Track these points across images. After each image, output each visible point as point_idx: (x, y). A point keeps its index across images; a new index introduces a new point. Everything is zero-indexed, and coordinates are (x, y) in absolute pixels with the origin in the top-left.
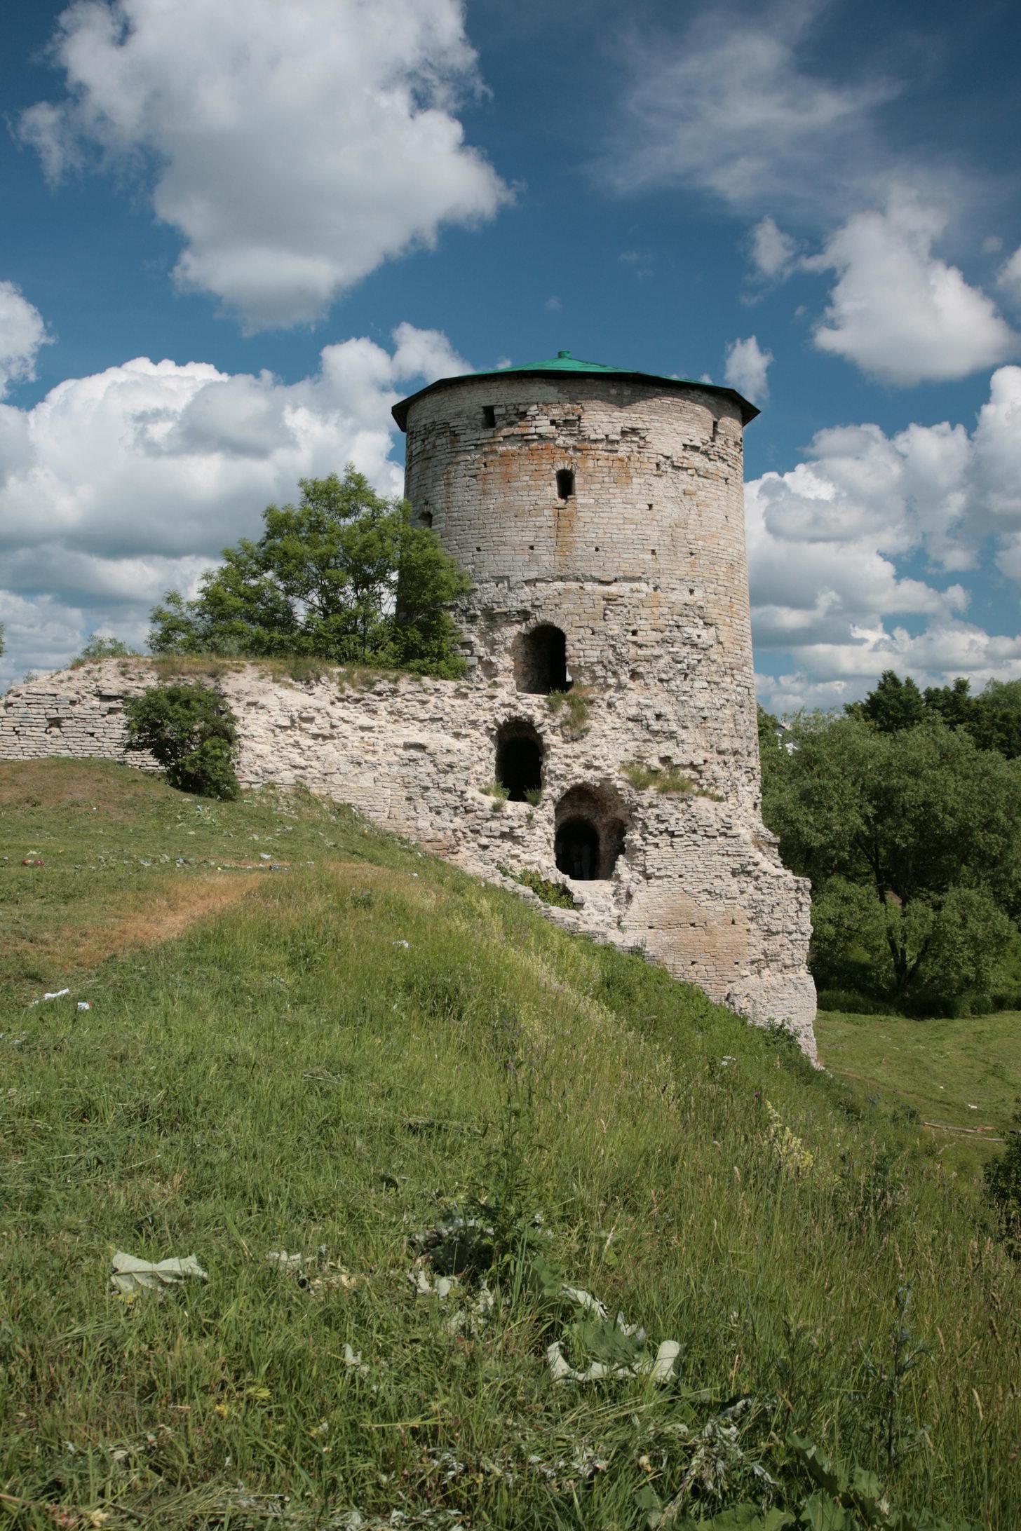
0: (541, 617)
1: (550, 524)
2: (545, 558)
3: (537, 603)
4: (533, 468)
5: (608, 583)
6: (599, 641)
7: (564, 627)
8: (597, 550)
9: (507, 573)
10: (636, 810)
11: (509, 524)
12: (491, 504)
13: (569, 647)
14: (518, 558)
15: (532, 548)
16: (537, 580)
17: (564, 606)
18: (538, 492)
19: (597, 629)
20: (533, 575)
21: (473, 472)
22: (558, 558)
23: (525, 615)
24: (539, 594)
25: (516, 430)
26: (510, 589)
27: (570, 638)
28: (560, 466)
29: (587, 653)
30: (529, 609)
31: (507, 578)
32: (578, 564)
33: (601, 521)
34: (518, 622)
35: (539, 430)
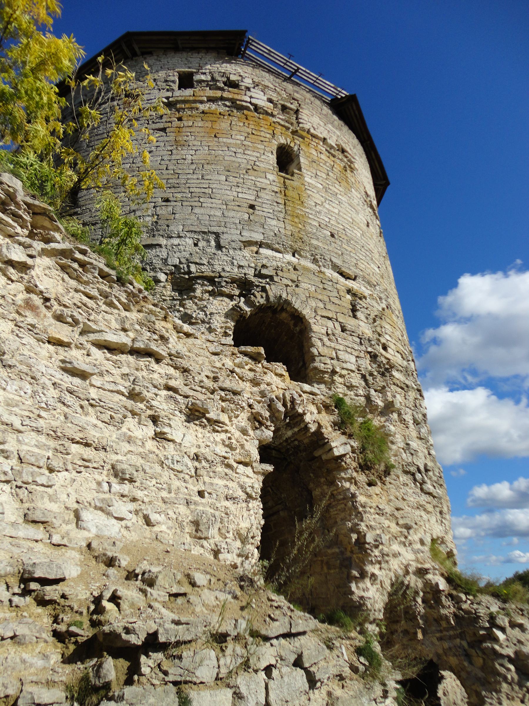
0: (273, 291)
1: (276, 189)
2: (274, 222)
3: (264, 271)
4: (250, 131)
5: (347, 277)
6: (351, 341)
7: (307, 312)
8: (332, 235)
9: (215, 229)
10: (496, 640)
11: (215, 177)
12: (188, 154)
13: (315, 341)
14: (231, 214)
15: (252, 207)
16: (261, 245)
17: (302, 285)
18: (258, 155)
19: (349, 327)
20: (258, 237)
21: (161, 126)
22: (289, 227)
23: (245, 286)
24: (265, 262)
25: (226, 95)
26: (219, 247)
27: (318, 328)
28: (283, 141)
29: (342, 355)
30: (253, 279)
31: (217, 235)
32: (314, 242)
33: (331, 208)
34: (231, 297)
35: (253, 101)
